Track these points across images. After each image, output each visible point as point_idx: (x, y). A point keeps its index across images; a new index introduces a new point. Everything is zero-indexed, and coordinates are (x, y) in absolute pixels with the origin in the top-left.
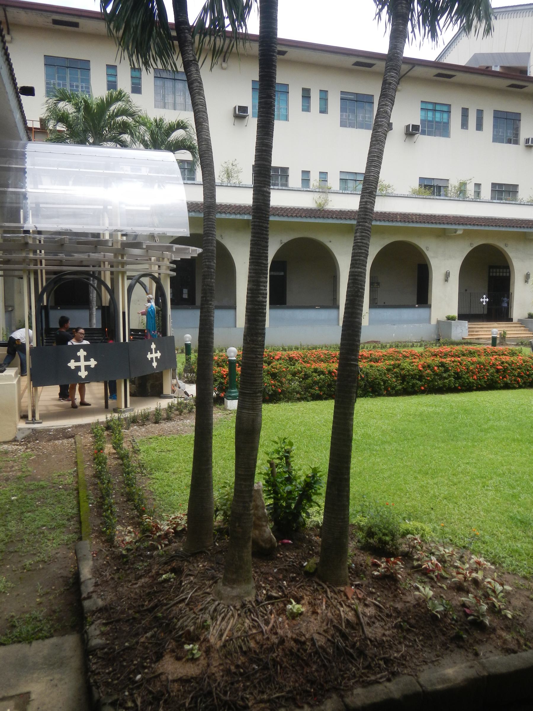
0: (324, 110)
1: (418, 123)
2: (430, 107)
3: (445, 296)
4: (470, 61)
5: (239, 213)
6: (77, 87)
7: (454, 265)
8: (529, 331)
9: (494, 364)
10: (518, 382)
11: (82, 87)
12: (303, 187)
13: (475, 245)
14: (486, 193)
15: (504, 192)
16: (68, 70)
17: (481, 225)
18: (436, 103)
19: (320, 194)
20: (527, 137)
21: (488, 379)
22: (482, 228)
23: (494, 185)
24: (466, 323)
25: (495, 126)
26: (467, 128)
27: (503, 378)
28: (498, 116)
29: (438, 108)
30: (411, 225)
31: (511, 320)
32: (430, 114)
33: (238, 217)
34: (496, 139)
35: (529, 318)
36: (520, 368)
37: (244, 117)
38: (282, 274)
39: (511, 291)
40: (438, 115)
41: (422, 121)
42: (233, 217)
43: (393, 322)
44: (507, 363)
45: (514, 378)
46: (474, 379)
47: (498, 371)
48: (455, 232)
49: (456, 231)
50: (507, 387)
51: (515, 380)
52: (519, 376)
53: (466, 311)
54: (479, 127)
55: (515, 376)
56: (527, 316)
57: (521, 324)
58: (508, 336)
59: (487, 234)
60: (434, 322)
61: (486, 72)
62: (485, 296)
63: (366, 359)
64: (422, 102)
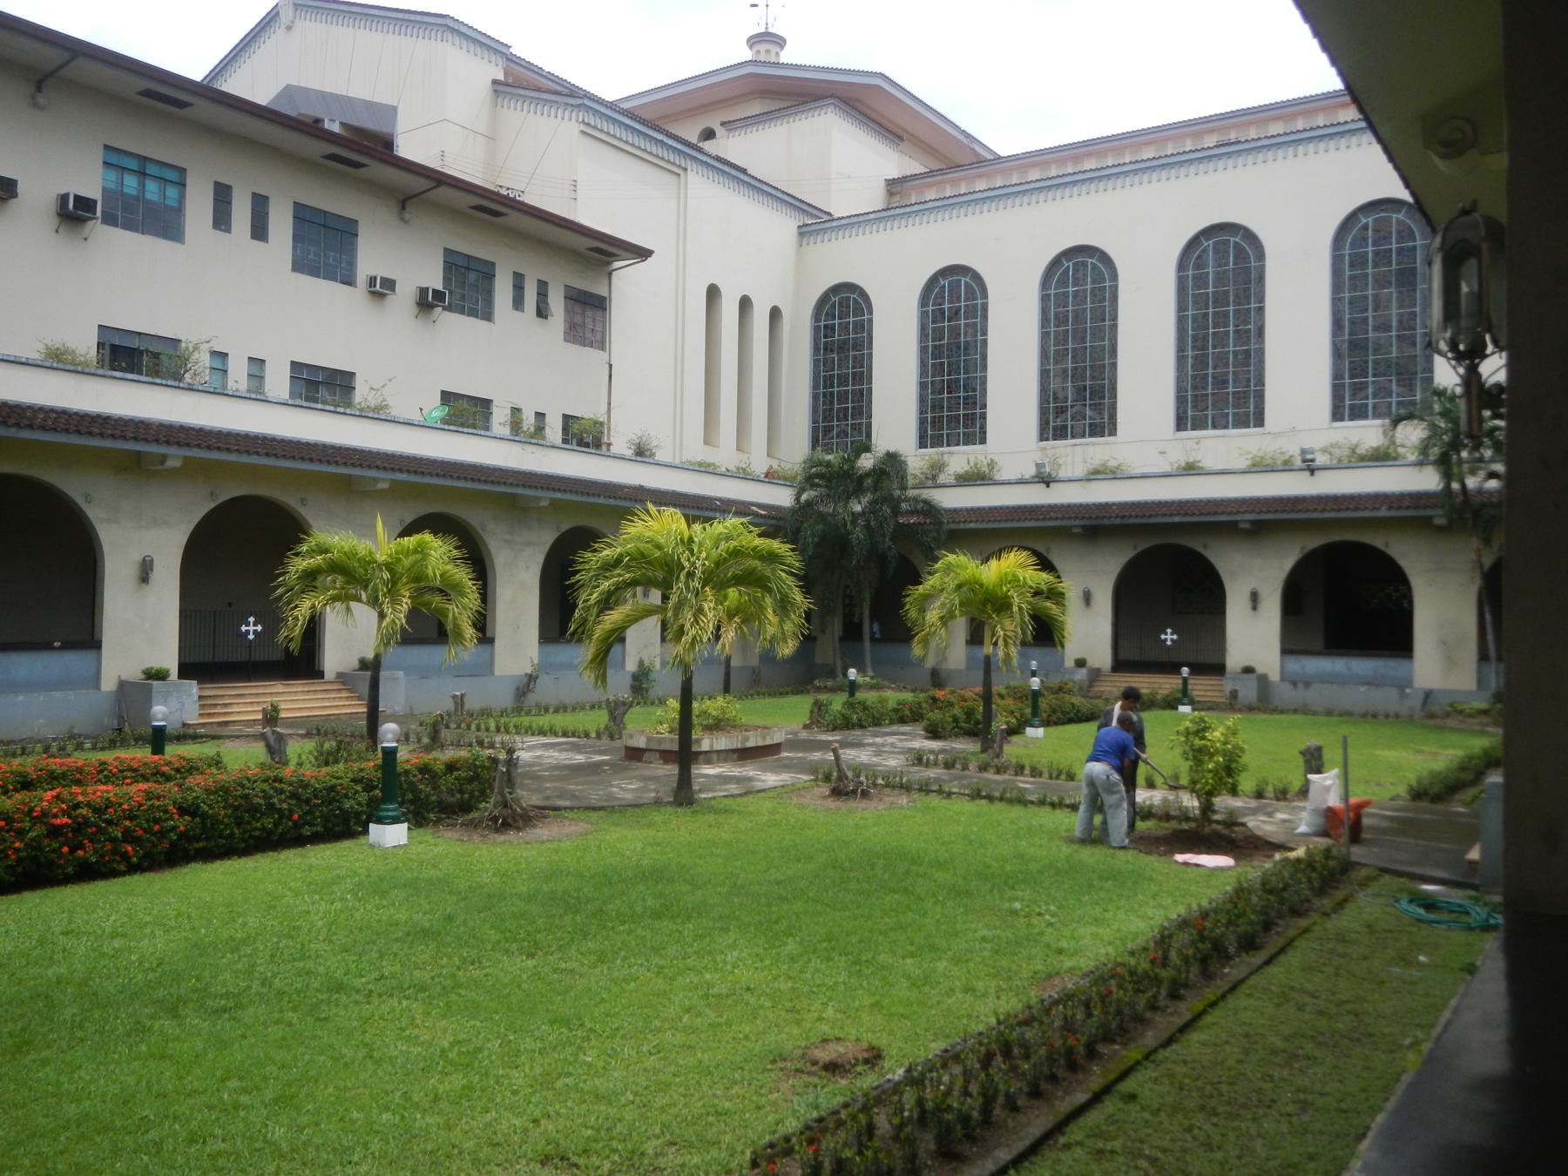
1: (93, 192)
2: (132, 164)
3: (142, 623)
4: (279, 97)
7: (167, 544)
9: (44, 814)
10: (125, 857)
13: (224, 497)
14: (278, 382)
15: (322, 385)
17: (228, 450)
18: (145, 158)
21: (19, 860)
22: (233, 457)
23: (295, 365)
24: (192, 687)
25: (297, 238)
26: (228, 230)
27: (73, 850)
28: (305, 218)
29: (151, 169)
30: (26, 434)
31: (319, 674)
32: (131, 182)
34: (299, 266)
36: (131, 819)
40: (152, 188)
41: (104, 190)
44: (88, 805)
45: (109, 846)
47: (55, 832)
48: (163, 463)
49: (163, 458)
50: (88, 873)
51: (114, 852)
53: (207, 657)
54: (259, 231)
55: (113, 840)
56: (356, 664)
57: (343, 683)
58: (283, 715)
59: (255, 472)
60: (108, 684)
61: (312, 128)
62: (252, 619)
64: (106, 147)
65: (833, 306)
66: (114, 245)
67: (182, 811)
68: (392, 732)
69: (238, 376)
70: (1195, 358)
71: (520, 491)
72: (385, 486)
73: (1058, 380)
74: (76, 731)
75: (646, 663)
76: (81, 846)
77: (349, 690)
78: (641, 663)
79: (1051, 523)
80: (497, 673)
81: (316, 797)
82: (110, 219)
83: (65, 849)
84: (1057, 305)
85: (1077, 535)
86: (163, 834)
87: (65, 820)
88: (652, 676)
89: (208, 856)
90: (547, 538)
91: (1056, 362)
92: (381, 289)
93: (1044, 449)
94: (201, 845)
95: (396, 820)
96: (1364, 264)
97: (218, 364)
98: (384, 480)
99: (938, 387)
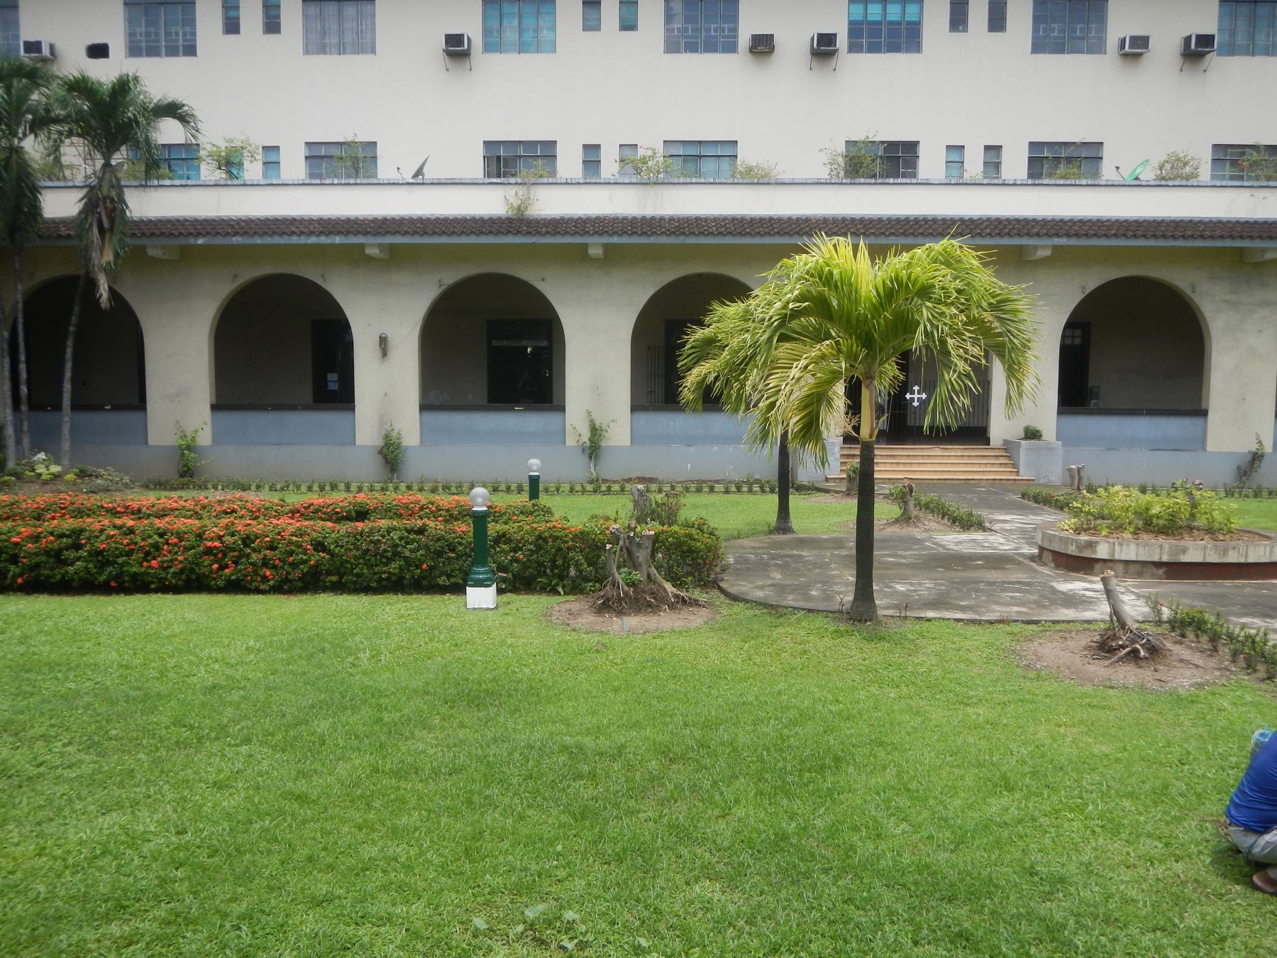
0: (628, 25)
5: (321, 233)
6: (177, 34)
8: (1014, 465)
11: (185, 34)
12: (585, 176)
14: (1015, 164)
16: (162, 8)
19: (516, 187)
20: (1122, 36)
25: (1037, 19)
27: (222, 568)
30: (692, 240)
31: (986, 441)
33: (323, 240)
34: (1037, 48)
36: (273, 548)
37: (465, 55)
38: (545, 343)
41: (851, 23)
42: (312, 240)
43: (689, 441)
46: (153, 568)
50: (236, 587)
52: (265, 563)
63: (133, 513)
66: (862, 70)
67: (319, 546)
68: (483, 497)
69: (974, 164)
71: (1246, 244)
72: (1047, 253)
74: (757, 477)
76: (227, 566)
80: (1209, 449)
81: (453, 550)
82: (854, 48)
83: (216, 566)
86: (294, 565)
87: (217, 543)
89: (339, 588)
92: (1135, 49)
94: (334, 578)
95: (480, 584)
97: (955, 156)
98: (1044, 247)
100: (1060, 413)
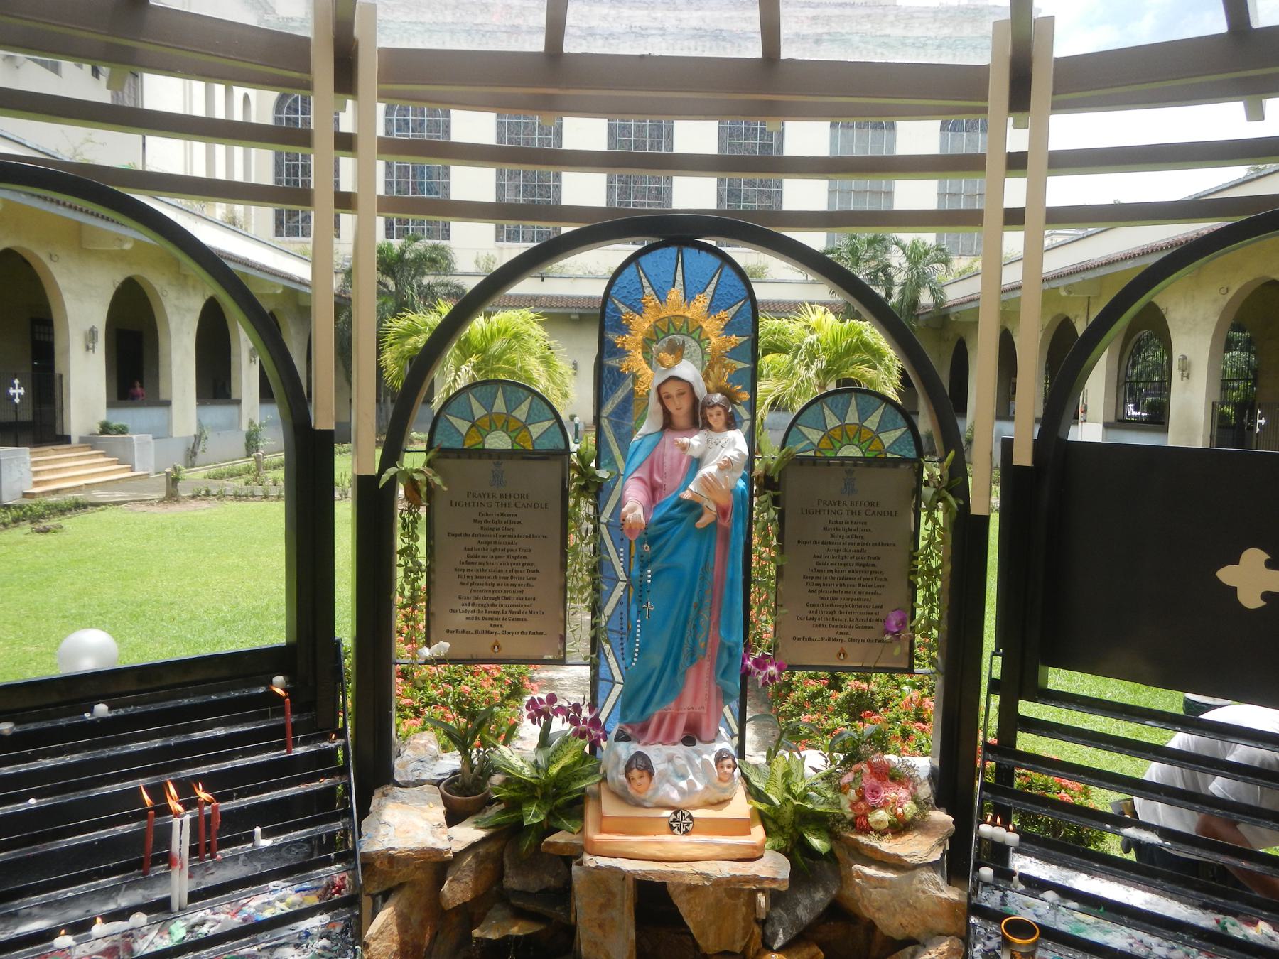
31: (66, 440)
35: (103, 433)
39: (59, 368)
56: (97, 429)
65: (296, 100)
70: (621, 189)
73: (512, 194)
75: (257, 422)
77: (105, 455)
78: (251, 423)
79: (556, 311)
80: (174, 435)
84: (510, 132)
85: (574, 321)
88: (262, 435)
90: (197, 304)
91: (510, 179)
93: (501, 248)
96: (739, 137)
99: (403, 187)
100: (110, 405)
